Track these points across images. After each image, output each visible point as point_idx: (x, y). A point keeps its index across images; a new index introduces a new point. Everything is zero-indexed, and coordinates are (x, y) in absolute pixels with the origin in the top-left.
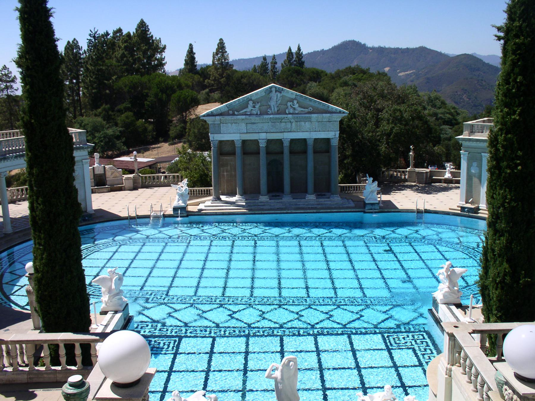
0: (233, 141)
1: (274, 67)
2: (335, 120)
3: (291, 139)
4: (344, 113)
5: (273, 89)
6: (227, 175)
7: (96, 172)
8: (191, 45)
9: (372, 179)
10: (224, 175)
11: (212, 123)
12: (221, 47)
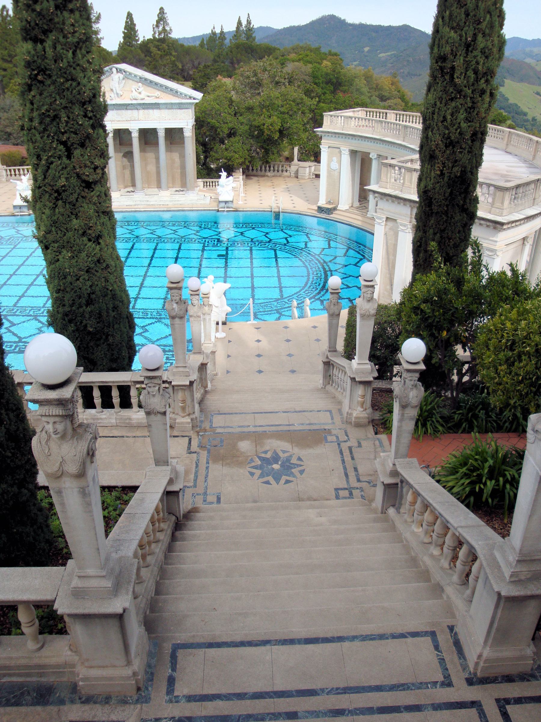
1: (222, 44)
5: (114, 70)
8: (130, 16)
12: (162, 18)
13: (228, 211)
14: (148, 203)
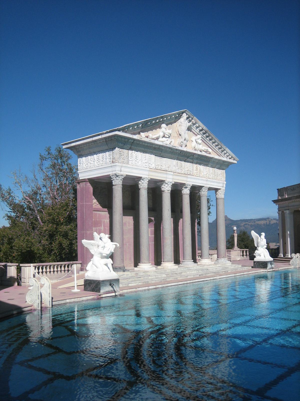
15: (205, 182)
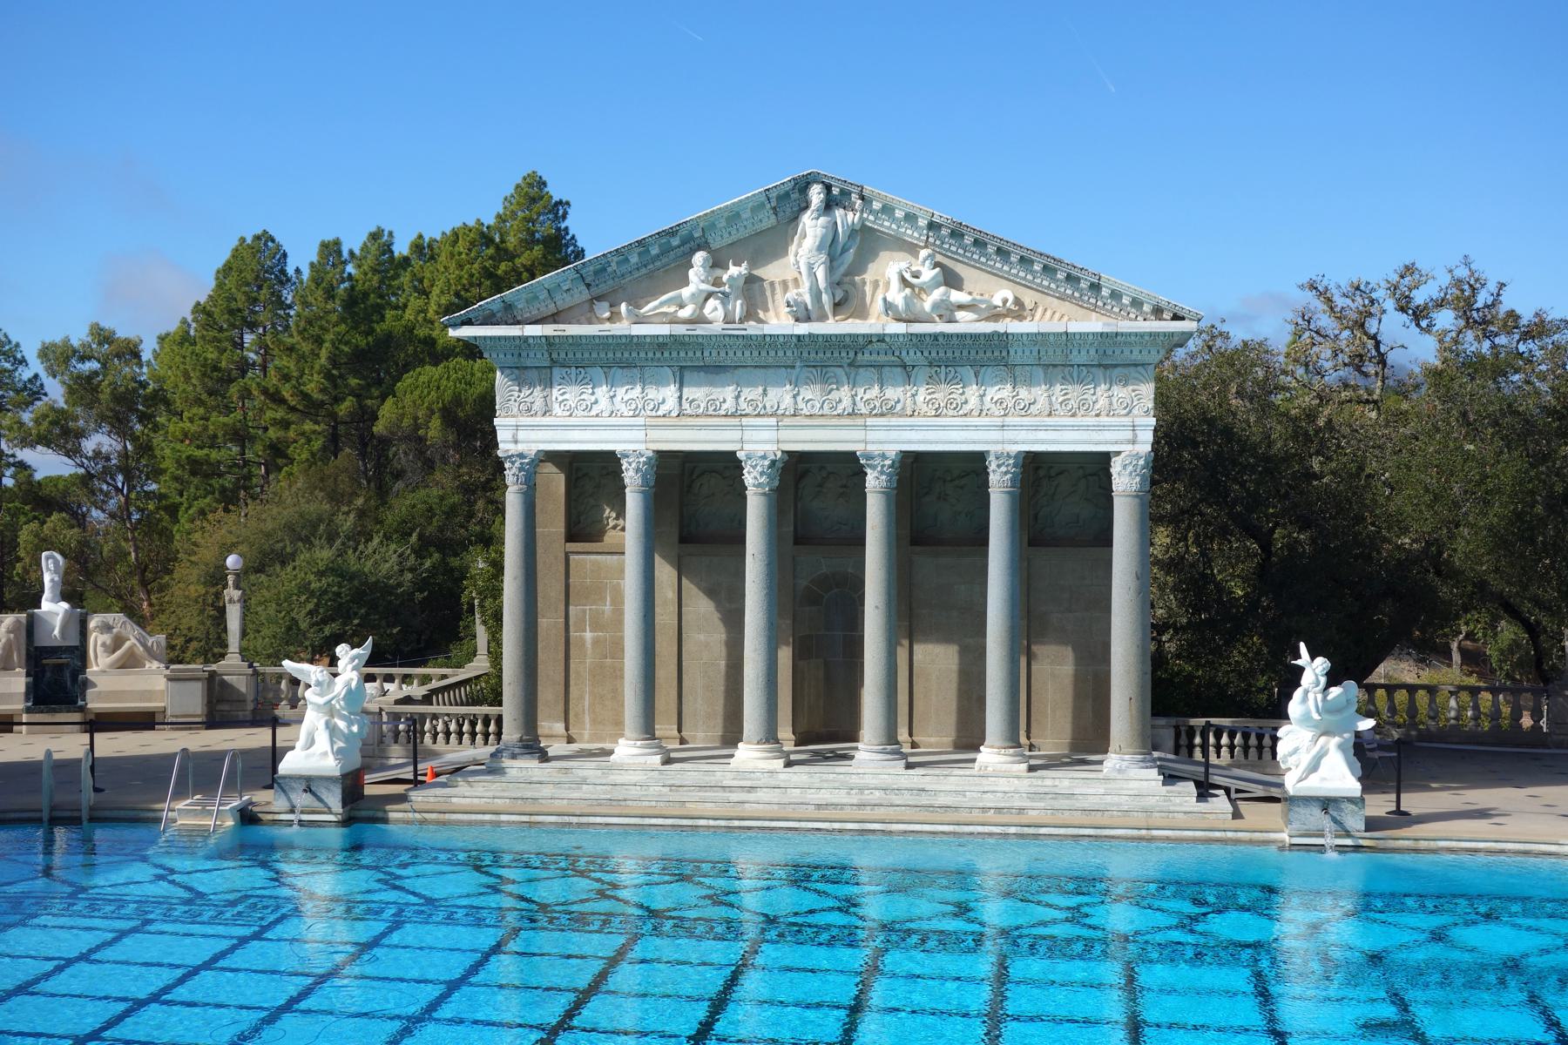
0: (612, 453)
2: (1136, 356)
3: (905, 455)
4: (1176, 317)
6: (596, 642)
7: (42, 641)
9: (1322, 664)
10: (582, 640)
11: (510, 360)
13: (1341, 849)
14: (924, 800)
15: (995, 435)
